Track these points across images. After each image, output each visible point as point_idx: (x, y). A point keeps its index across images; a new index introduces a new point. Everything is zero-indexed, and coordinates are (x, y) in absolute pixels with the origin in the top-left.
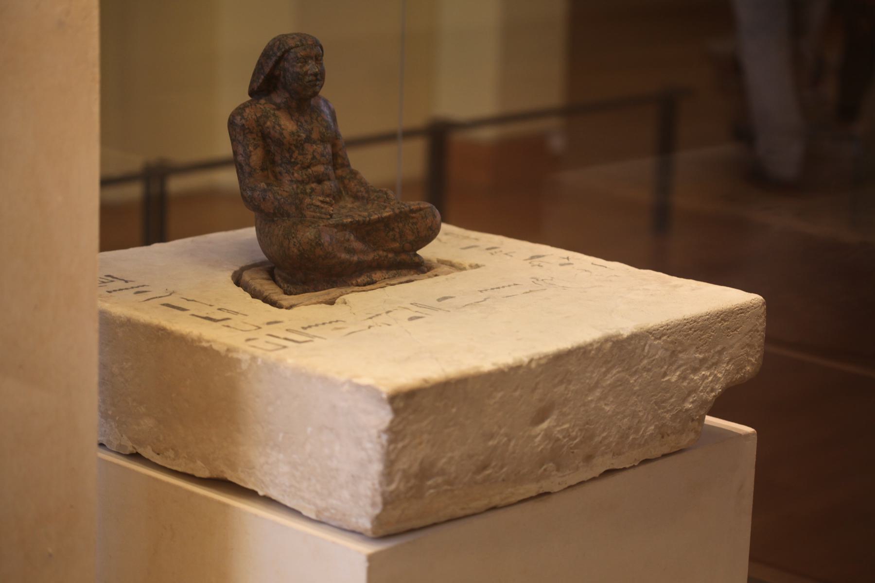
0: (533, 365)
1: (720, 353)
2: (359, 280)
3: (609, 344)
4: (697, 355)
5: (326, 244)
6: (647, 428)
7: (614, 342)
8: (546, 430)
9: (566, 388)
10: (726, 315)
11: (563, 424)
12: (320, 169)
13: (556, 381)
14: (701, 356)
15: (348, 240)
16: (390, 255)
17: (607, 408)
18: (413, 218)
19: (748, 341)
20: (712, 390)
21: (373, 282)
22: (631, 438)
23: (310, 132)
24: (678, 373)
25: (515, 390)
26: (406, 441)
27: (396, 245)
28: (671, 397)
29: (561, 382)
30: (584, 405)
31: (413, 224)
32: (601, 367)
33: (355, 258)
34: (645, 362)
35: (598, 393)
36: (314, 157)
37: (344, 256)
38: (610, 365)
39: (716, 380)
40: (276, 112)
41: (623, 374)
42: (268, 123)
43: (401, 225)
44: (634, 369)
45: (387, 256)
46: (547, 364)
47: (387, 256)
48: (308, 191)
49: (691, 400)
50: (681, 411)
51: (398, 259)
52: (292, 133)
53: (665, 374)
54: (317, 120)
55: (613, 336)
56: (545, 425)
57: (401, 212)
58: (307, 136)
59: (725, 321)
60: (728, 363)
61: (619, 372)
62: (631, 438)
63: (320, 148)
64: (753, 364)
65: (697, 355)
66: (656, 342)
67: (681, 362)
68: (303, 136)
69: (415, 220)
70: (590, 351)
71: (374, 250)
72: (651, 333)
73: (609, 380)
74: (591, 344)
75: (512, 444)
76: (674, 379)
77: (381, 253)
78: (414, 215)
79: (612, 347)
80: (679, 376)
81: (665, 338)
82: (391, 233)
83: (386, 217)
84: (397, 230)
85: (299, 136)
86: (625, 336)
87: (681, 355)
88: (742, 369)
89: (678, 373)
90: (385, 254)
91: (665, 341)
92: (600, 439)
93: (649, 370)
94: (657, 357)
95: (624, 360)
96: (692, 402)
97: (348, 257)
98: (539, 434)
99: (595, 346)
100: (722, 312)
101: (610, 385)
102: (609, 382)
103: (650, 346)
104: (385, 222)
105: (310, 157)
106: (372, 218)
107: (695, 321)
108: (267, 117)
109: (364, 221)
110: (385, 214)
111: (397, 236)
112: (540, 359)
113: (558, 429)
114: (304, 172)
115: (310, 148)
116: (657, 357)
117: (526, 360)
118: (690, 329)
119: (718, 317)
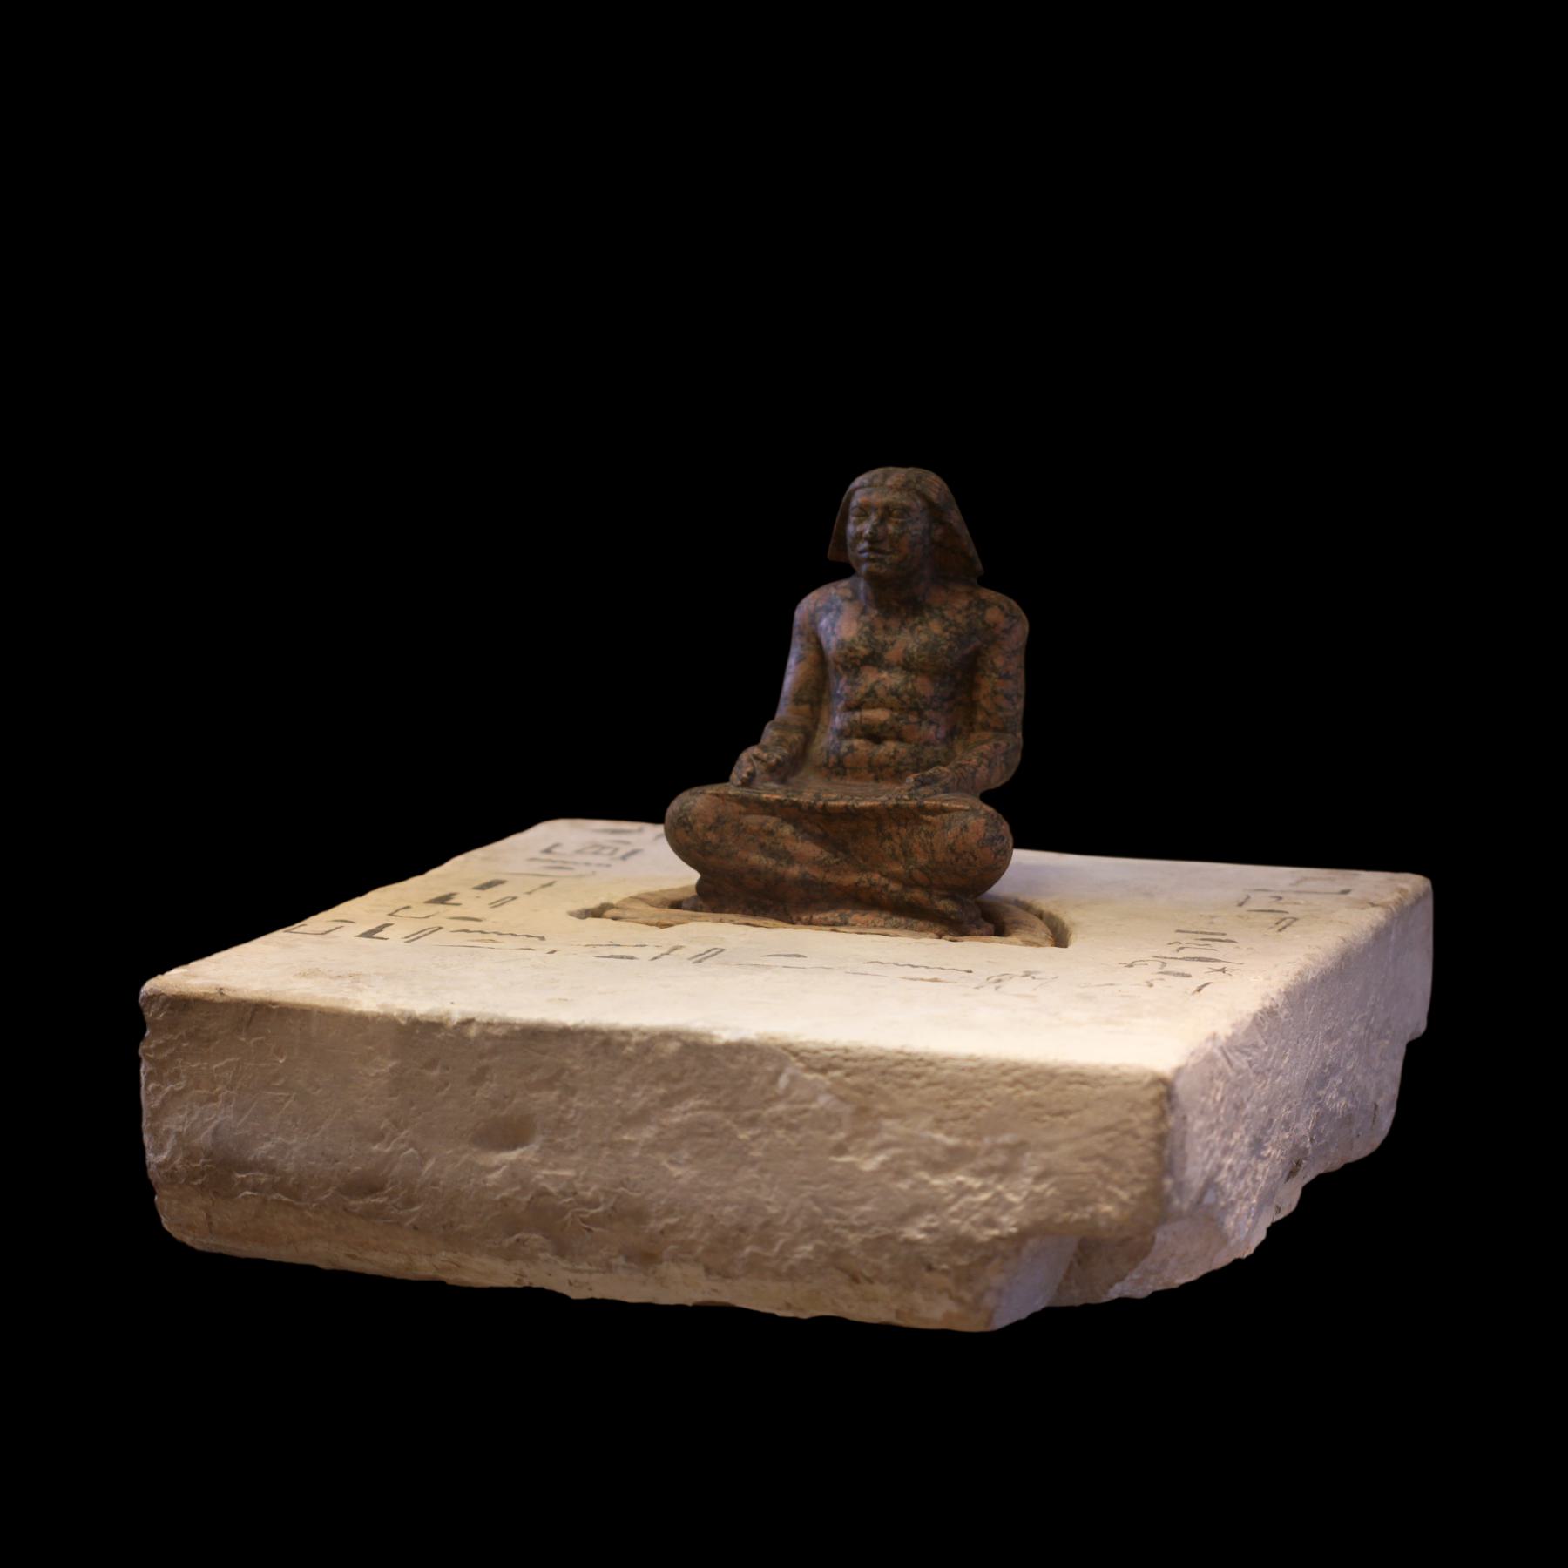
0: (473, 1032)
1: (1017, 1149)
2: (816, 917)
3: (673, 1046)
4: (939, 1136)
5: (699, 825)
6: (794, 1243)
7: (686, 1045)
8: (512, 1164)
9: (560, 1100)
10: (1029, 1076)
11: (557, 1166)
12: (880, 715)
13: (534, 1077)
14: (951, 1141)
15: (771, 833)
16: (894, 887)
17: (677, 1171)
18: (929, 823)
19: (1103, 1149)
20: (990, 1223)
21: (845, 924)
22: (748, 1250)
23: (885, 647)
24: (881, 1158)
25: (431, 1064)
26: (181, 1085)
27: (898, 868)
28: (862, 1201)
29: (549, 1083)
30: (612, 1145)
31: (928, 834)
32: (656, 1083)
33: (794, 871)
34: (780, 1108)
35: (648, 1133)
36: (872, 692)
37: (756, 859)
38: (677, 1087)
39: (998, 1202)
40: (846, 606)
41: (717, 1115)
42: (824, 623)
43: (903, 831)
44: (747, 1114)
45: (886, 886)
46: (505, 1037)
47: (886, 886)
48: (844, 750)
49: (923, 1224)
50: (892, 1237)
51: (908, 896)
52: (842, 643)
53: (840, 1149)
54: (912, 630)
55: (689, 1034)
56: (512, 1155)
57: (897, 806)
58: (873, 653)
59: (1028, 1087)
60: (1039, 1178)
61: (701, 1107)
62: (748, 1250)
63: (892, 679)
64: (1123, 1204)
65: (939, 1136)
66: (810, 1076)
67: (887, 1137)
68: (863, 651)
69: (930, 829)
70: (622, 1045)
71: (864, 870)
72: (795, 1054)
73: (679, 1115)
74: (625, 1032)
75: (430, 1165)
76: (870, 1165)
77: (876, 877)
78: (930, 818)
79: (680, 1051)
80: (883, 1164)
81: (837, 1074)
82: (887, 844)
83: (864, 809)
84: (897, 840)
85: (851, 649)
86: (721, 1041)
87: (888, 1123)
88: (1085, 1204)
89: (881, 1158)
90: (884, 881)
91: (838, 1082)
92: (661, 1225)
93: (791, 1128)
94: (814, 1106)
95: (716, 1088)
96: (928, 1230)
97: (771, 862)
98: (498, 1168)
99: (635, 1039)
100: (1017, 1067)
101: (679, 1126)
102: (677, 1120)
103: (793, 1078)
104: (880, 817)
105: (862, 690)
106: (832, 803)
107: (930, 1064)
108: (828, 610)
109: (811, 809)
110: (863, 804)
111: (898, 851)
112: (489, 1024)
113: (545, 1172)
114: (848, 715)
115: (870, 677)
116: (814, 1106)
117: (456, 1018)
118: (917, 1076)
119: (1005, 1073)
